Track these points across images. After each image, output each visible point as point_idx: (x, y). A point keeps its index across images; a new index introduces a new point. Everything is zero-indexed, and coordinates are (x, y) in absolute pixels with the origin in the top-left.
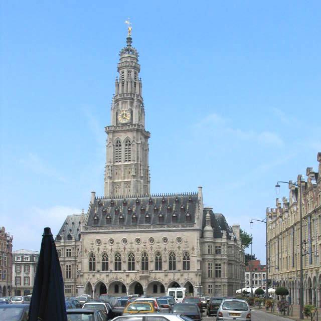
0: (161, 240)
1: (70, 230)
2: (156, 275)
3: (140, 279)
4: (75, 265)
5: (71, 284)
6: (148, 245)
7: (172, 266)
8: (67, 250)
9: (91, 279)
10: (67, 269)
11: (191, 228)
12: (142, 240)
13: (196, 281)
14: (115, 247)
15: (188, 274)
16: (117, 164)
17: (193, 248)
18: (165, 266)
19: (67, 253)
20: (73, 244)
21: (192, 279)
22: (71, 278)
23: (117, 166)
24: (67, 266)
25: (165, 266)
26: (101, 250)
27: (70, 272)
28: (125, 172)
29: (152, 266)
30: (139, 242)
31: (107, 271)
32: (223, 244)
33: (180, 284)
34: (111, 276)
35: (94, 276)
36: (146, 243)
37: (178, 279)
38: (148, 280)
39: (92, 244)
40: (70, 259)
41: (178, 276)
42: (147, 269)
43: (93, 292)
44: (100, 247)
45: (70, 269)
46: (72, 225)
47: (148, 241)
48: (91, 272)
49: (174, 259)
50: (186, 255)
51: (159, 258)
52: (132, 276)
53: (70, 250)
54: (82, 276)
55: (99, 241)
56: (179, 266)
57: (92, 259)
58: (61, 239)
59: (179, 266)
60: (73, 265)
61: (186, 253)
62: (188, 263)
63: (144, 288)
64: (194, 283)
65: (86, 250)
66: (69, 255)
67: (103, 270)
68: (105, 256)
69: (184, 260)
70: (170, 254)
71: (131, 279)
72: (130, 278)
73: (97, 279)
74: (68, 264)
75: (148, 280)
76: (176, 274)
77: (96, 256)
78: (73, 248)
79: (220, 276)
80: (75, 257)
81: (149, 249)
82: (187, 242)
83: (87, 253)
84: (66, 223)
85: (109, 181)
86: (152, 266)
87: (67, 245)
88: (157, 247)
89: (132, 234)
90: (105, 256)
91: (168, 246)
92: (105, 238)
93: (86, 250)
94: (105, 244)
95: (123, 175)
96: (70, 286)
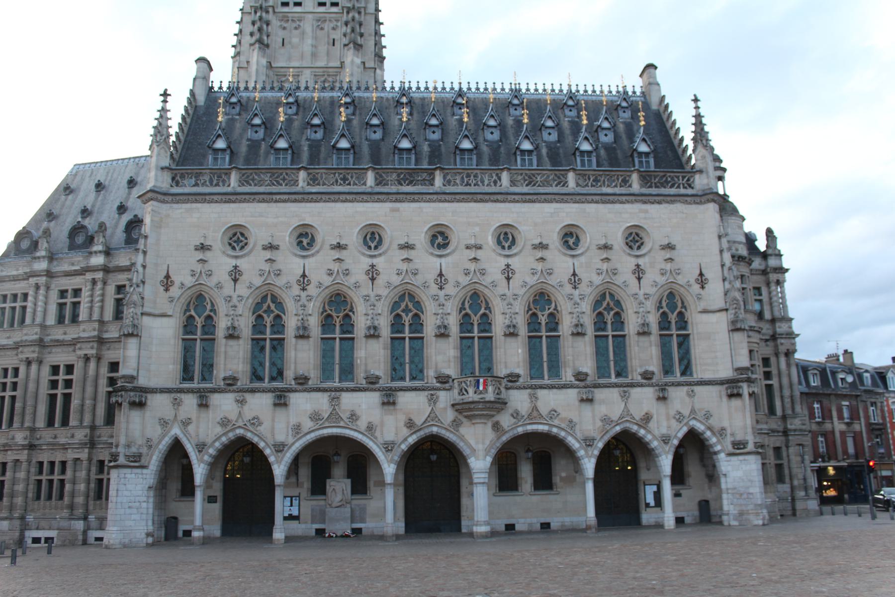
0: (554, 239)
1: (85, 212)
2: (534, 398)
3: (456, 424)
4: (99, 359)
5: (70, 455)
6: (493, 262)
7: (612, 360)
8: (63, 293)
9: (186, 423)
10: (54, 384)
11: (682, 191)
12: (460, 236)
13: (735, 419)
14: (319, 266)
15: (691, 395)
16: (286, 9)
17: (701, 274)
18: (579, 355)
19: (61, 306)
20: (98, 260)
21: (708, 416)
22: (73, 422)
23: (285, 18)
24: (55, 369)
25: (579, 355)
26: (244, 279)
27: (67, 397)
28: (315, 38)
29: (511, 356)
30: (445, 246)
31: (275, 384)
32: (773, 277)
33: (655, 444)
34: (303, 404)
35: (203, 405)
36: (480, 248)
37: (647, 418)
38: (496, 427)
39: (202, 248)
40: (72, 333)
41: (643, 399)
42: (488, 370)
43: (199, 495)
44: (243, 264)
45: (68, 384)
46: (93, 195)
47: (490, 241)
48: (186, 385)
49: (619, 322)
50: (672, 307)
51: (543, 319)
52: (413, 403)
53: (77, 292)
54: (140, 405)
55: (237, 238)
56: (644, 355)
57: (199, 321)
58: (35, 245)
59: (644, 355)
60: (87, 359)
61: (671, 295)
62: (684, 340)
63: (480, 464)
64: (722, 432)
65: (168, 277)
66: (68, 313)
67: (256, 376)
68: (268, 307)
69: (661, 329)
70: (598, 303)
71: (410, 424)
72: (402, 419)
73: (225, 422)
74: (61, 357)
75: (496, 427)
76: (635, 392)
77: (222, 308)
78: (94, 282)
79: (772, 410)
80: (101, 322)
81: (500, 278)
82: (670, 247)
83: (175, 291)
84: (66, 189)
85: (255, 58)
86: (511, 356)
87: (66, 267)
88: (539, 266)
89: (407, 208)
90: (268, 307)
91: (589, 266)
92: (270, 220)
93: (168, 277)
94: (271, 247)
95: (307, 47)
96: (64, 464)
